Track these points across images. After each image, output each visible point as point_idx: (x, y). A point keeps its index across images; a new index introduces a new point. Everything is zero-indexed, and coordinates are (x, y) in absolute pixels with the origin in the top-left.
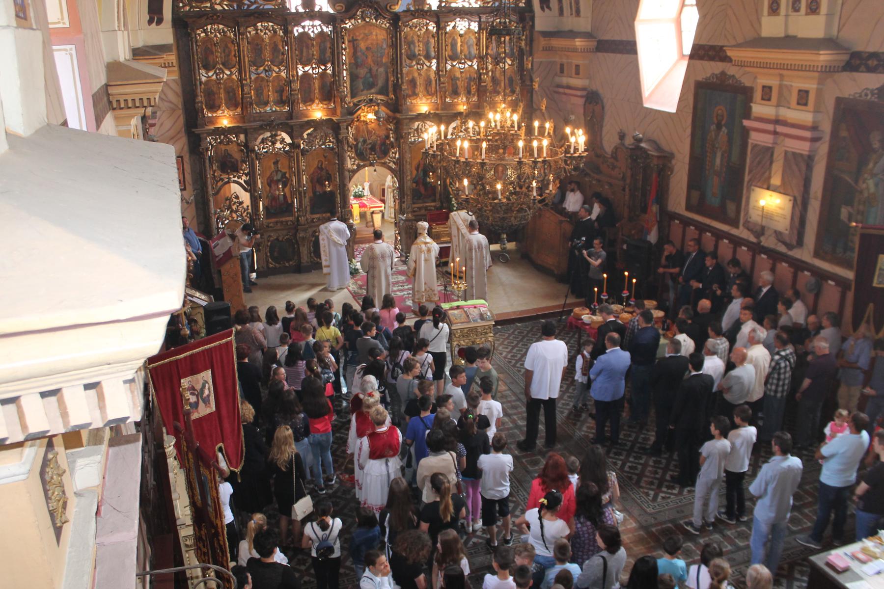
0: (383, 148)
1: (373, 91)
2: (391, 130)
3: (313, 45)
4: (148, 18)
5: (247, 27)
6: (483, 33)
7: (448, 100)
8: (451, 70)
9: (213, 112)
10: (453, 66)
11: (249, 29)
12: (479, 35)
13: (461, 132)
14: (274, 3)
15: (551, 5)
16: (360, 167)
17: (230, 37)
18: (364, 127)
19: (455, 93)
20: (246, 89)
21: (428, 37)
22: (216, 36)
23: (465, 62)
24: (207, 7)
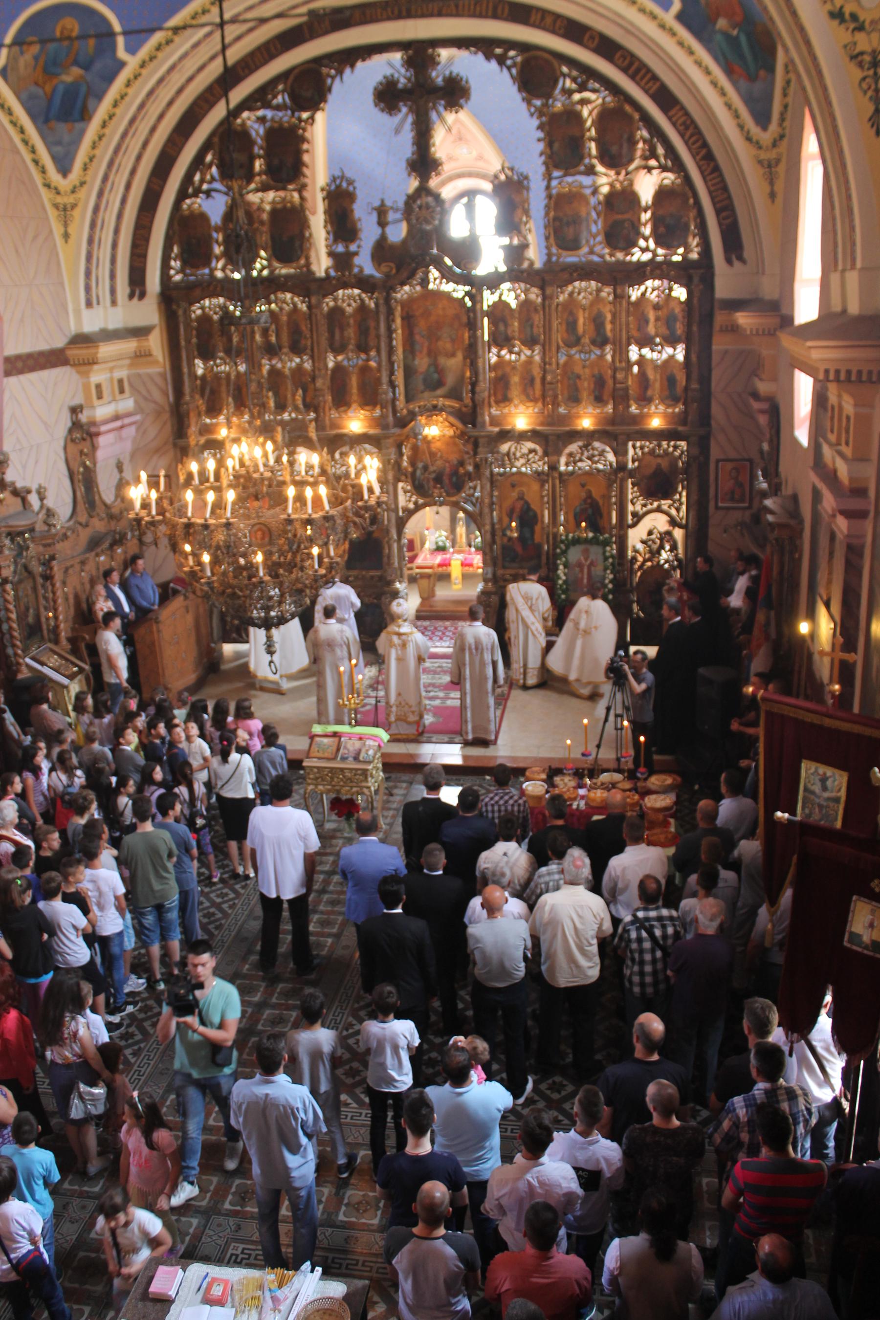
0: (454, 479)
1: (439, 392)
2: (468, 453)
3: (348, 325)
4: (128, 290)
7: (562, 410)
8: (566, 364)
9: (211, 418)
10: (570, 356)
13: (581, 460)
14: (294, 265)
15: (746, 254)
16: (418, 508)
18: (425, 447)
19: (575, 399)
20: (253, 387)
23: (590, 352)
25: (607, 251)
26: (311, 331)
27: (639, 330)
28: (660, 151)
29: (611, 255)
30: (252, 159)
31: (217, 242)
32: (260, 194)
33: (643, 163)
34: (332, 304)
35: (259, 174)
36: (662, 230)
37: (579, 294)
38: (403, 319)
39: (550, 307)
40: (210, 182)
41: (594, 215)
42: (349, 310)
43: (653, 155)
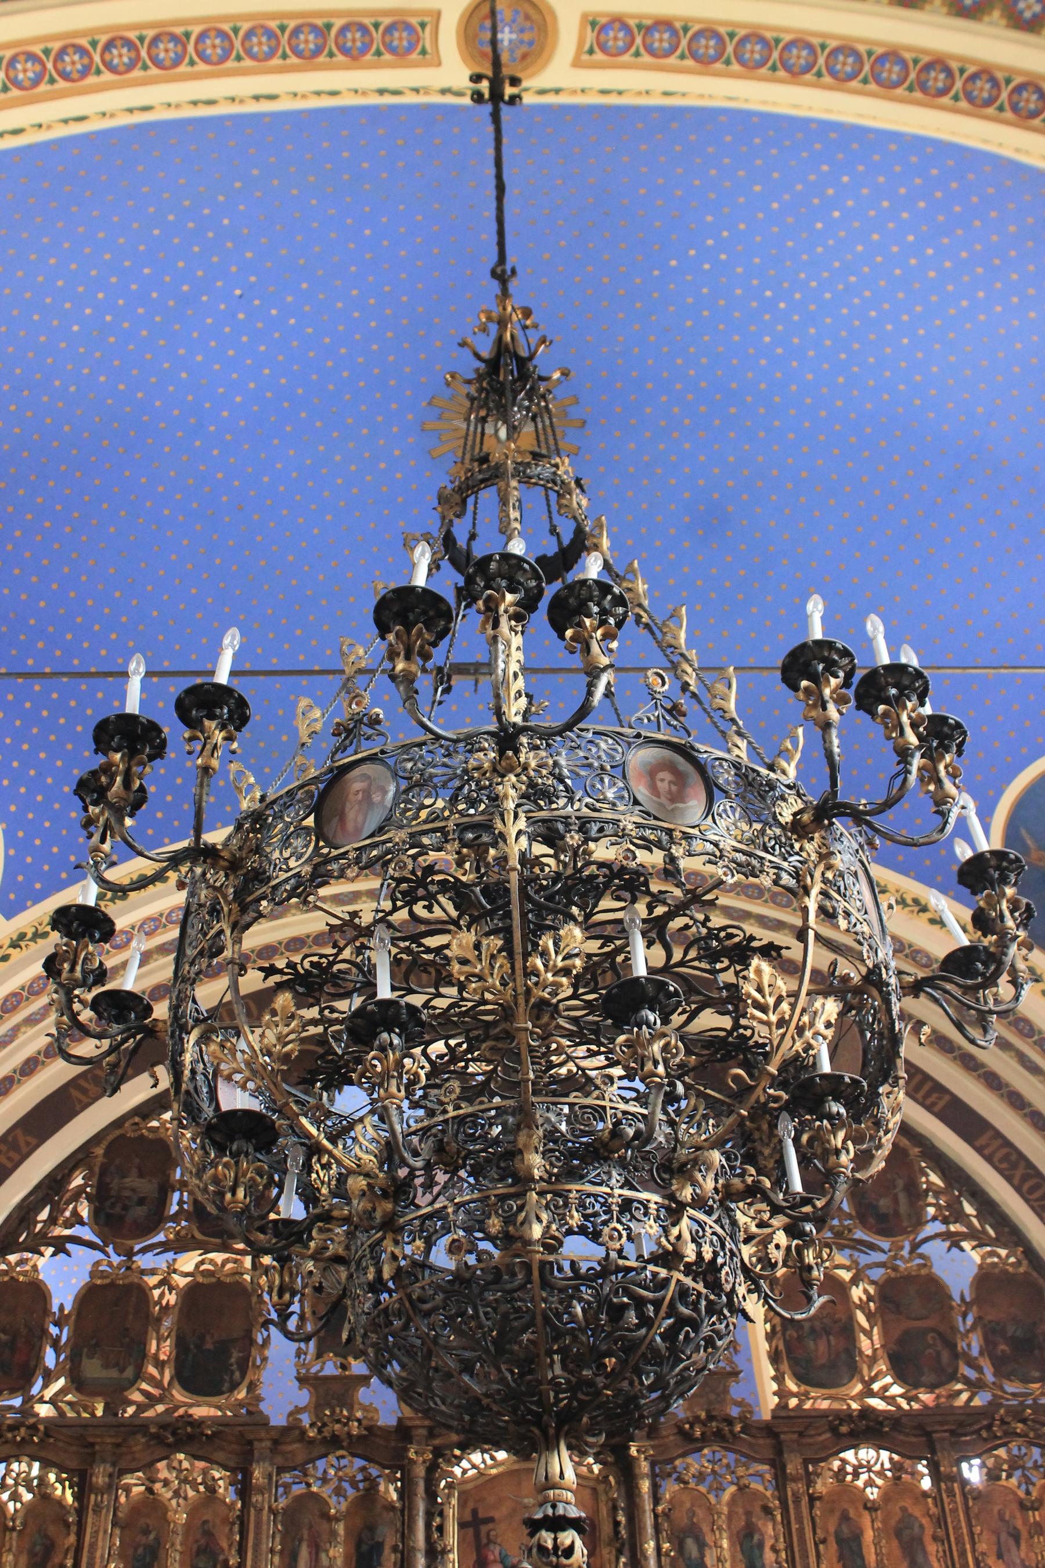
3: (334, 1534)
5: (123, 1472)
6: (951, 1493)
11: (128, 1480)
12: (938, 1500)
14: (222, 1400)
17: (60, 1503)
21: (748, 1514)
22: (15, 1497)
24: (11, 1408)
25: (896, 1390)
26: (242, 1551)
27: (1000, 1556)
28: (969, 1209)
29: (909, 1400)
30: (165, 1189)
31: (55, 1343)
32: (170, 1256)
33: (943, 1228)
34: (298, 1490)
35: (175, 1218)
36: (1003, 1347)
37: (856, 1475)
38: (462, 1525)
39: (797, 1501)
40: (68, 1225)
41: (861, 1318)
42: (336, 1506)
43: (960, 1216)
